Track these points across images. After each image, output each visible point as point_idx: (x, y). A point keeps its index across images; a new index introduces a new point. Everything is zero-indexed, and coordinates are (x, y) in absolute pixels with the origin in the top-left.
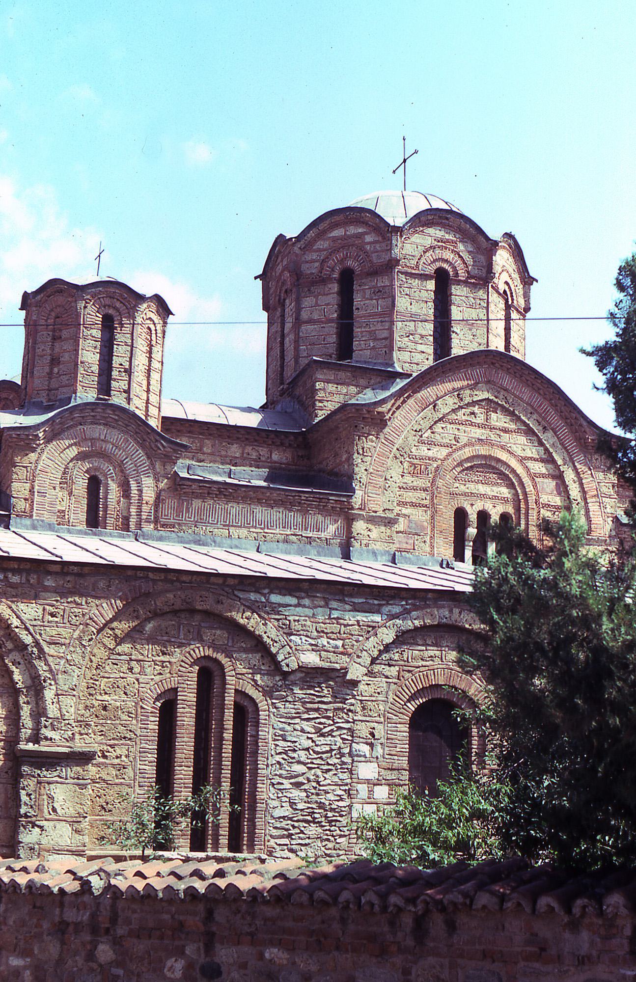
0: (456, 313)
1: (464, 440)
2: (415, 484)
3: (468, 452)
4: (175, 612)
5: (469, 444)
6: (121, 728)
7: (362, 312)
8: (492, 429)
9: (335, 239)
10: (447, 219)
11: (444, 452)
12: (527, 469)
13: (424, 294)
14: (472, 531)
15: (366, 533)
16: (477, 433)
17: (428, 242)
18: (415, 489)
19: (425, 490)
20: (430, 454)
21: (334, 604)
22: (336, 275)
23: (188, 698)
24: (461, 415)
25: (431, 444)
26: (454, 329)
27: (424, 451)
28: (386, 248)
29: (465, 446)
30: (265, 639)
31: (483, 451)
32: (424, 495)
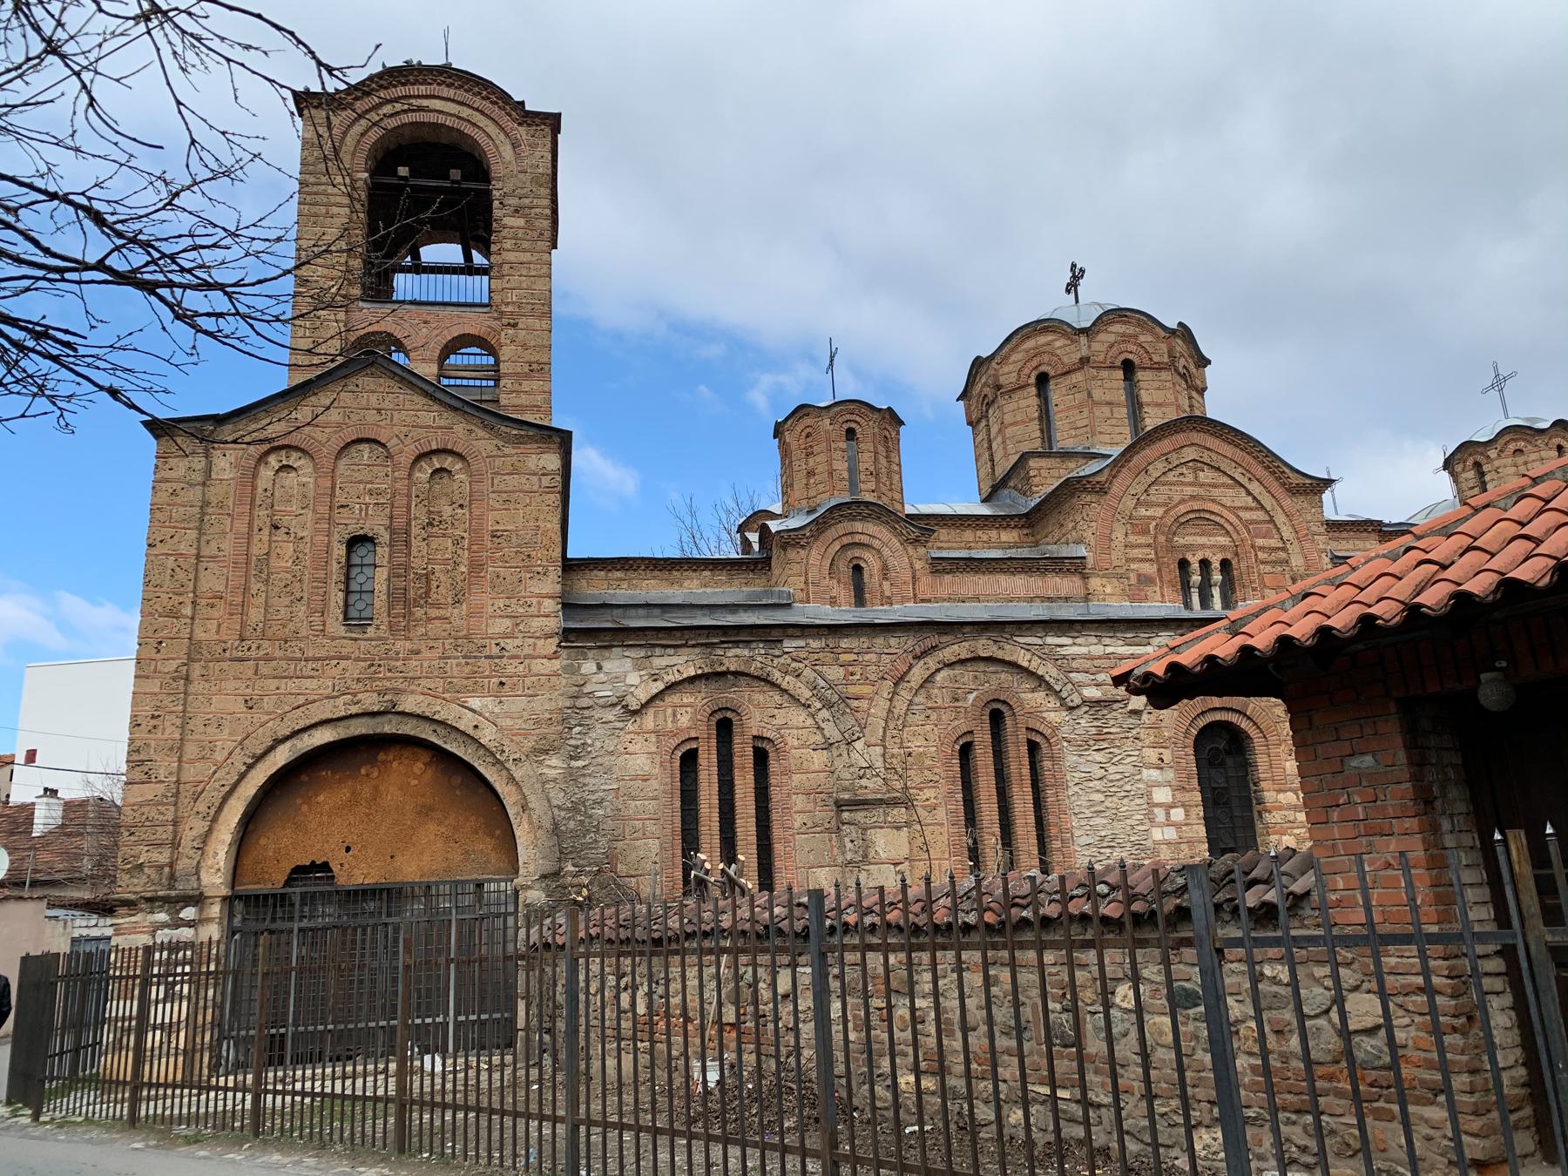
0: (1145, 397)
1: (1177, 499)
3: (1183, 509)
4: (962, 662)
5: (1182, 501)
6: (927, 772)
7: (1061, 407)
8: (1202, 485)
11: (1159, 512)
12: (1238, 517)
13: (1115, 384)
14: (1196, 578)
15: (1101, 589)
16: (1189, 490)
17: (1112, 338)
19: (1149, 546)
20: (1148, 514)
21: (1107, 641)
22: (1032, 380)
23: (983, 740)
24: (1171, 477)
25: (1149, 505)
27: (1142, 512)
29: (1180, 503)
30: (1047, 678)
32: (1147, 550)
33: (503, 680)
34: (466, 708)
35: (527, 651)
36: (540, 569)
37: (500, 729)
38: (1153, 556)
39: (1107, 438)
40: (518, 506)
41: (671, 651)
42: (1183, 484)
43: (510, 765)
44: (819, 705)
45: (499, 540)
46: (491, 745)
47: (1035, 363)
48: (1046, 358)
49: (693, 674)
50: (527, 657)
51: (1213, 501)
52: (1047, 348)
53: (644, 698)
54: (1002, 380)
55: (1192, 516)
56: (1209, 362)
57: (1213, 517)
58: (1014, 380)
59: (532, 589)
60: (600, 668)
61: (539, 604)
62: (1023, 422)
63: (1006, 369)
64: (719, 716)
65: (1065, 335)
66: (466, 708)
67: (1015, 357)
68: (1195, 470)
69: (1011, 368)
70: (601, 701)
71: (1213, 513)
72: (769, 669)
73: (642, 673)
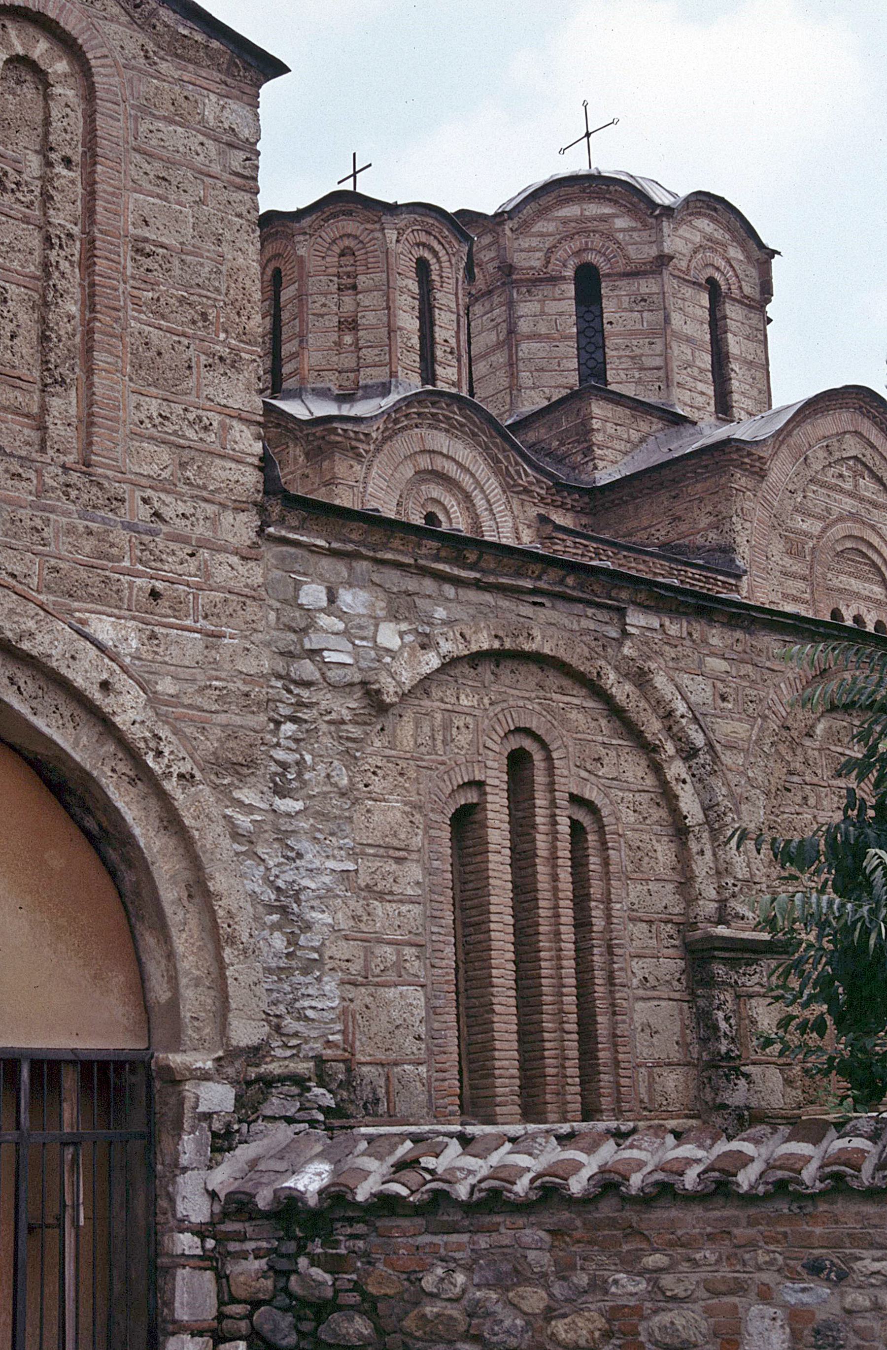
2: (794, 568)
7: (616, 328)
8: (862, 499)
9: (565, 221)
10: (715, 210)
17: (697, 238)
18: (794, 576)
20: (804, 526)
22: (569, 273)
26: (733, 366)
28: (649, 239)
31: (856, 530)
32: (801, 585)
33: (159, 585)
34: (86, 637)
35: (201, 530)
36: (225, 352)
37: (154, 700)
38: (807, 596)
39: (686, 396)
40: (184, 197)
41: (449, 591)
42: (841, 491)
43: (170, 786)
44: (670, 748)
45: (148, 263)
46: (137, 734)
47: (576, 245)
48: (597, 241)
49: (486, 646)
50: (203, 543)
51: (873, 527)
52: (602, 226)
53: (407, 678)
54: (519, 259)
55: (849, 544)
56: (770, 321)
57: (870, 553)
58: (537, 264)
59: (210, 391)
60: (332, 598)
61: (225, 428)
62: (548, 337)
63: (525, 243)
64: (515, 742)
65: (632, 211)
66: (86, 637)
67: (541, 226)
68: (856, 475)
69: (534, 242)
70: (334, 675)
71: (871, 545)
72: (602, 663)
73: (404, 626)
